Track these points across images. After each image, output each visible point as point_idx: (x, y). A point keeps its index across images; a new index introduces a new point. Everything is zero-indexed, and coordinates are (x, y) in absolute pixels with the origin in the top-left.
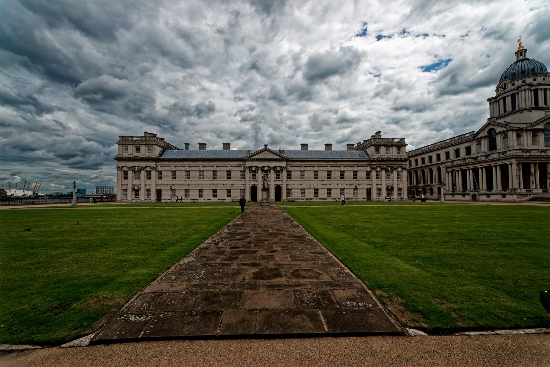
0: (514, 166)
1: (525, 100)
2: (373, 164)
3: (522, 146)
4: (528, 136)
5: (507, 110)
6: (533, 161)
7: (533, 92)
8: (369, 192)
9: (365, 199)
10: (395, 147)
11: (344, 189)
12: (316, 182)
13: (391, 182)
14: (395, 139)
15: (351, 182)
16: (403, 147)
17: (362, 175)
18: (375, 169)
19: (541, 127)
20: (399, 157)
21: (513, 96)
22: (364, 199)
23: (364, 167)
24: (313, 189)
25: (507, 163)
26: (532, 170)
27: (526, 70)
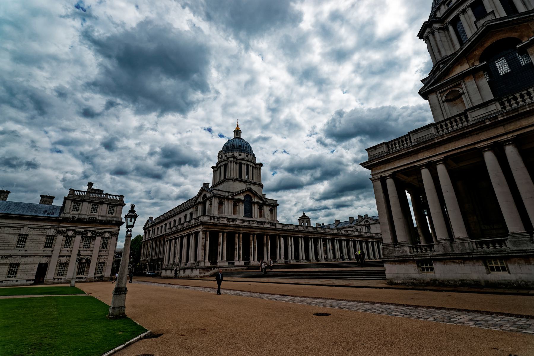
0: (201, 233)
1: (231, 170)
2: (61, 225)
3: (223, 214)
4: (229, 204)
5: (221, 179)
6: (221, 229)
7: (238, 165)
8: (42, 269)
9: (30, 280)
10: (106, 205)
13: (89, 253)
14: (110, 195)
15: (9, 252)
16: (118, 207)
18: (64, 233)
19: (241, 197)
20: (110, 219)
21: (225, 165)
22: (27, 280)
23: (45, 229)
25: (198, 230)
26: (220, 240)
27: (236, 145)
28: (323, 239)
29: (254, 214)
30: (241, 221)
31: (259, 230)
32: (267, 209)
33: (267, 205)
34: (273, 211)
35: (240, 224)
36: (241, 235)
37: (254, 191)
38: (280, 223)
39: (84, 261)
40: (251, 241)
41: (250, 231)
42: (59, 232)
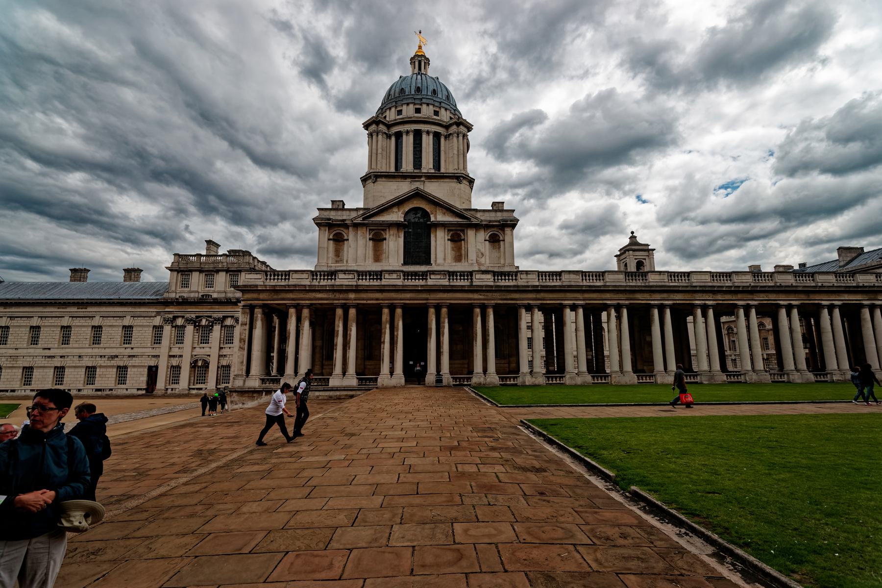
2: (166, 310)
6: (293, 299)
7: (393, 139)
8: (153, 372)
9: (141, 389)
11: (95, 368)
12: (32, 351)
13: (206, 351)
15: (114, 350)
17: (143, 335)
19: (397, 216)
22: (138, 389)
24: (19, 367)
28: (756, 307)
29: (436, 254)
30: (351, 276)
31: (408, 295)
32: (476, 241)
33: (477, 227)
34: (499, 241)
35: (350, 283)
36: (352, 312)
37: (430, 195)
38: (520, 269)
39: (200, 364)
40: (383, 326)
41: (377, 299)
42: (166, 321)
